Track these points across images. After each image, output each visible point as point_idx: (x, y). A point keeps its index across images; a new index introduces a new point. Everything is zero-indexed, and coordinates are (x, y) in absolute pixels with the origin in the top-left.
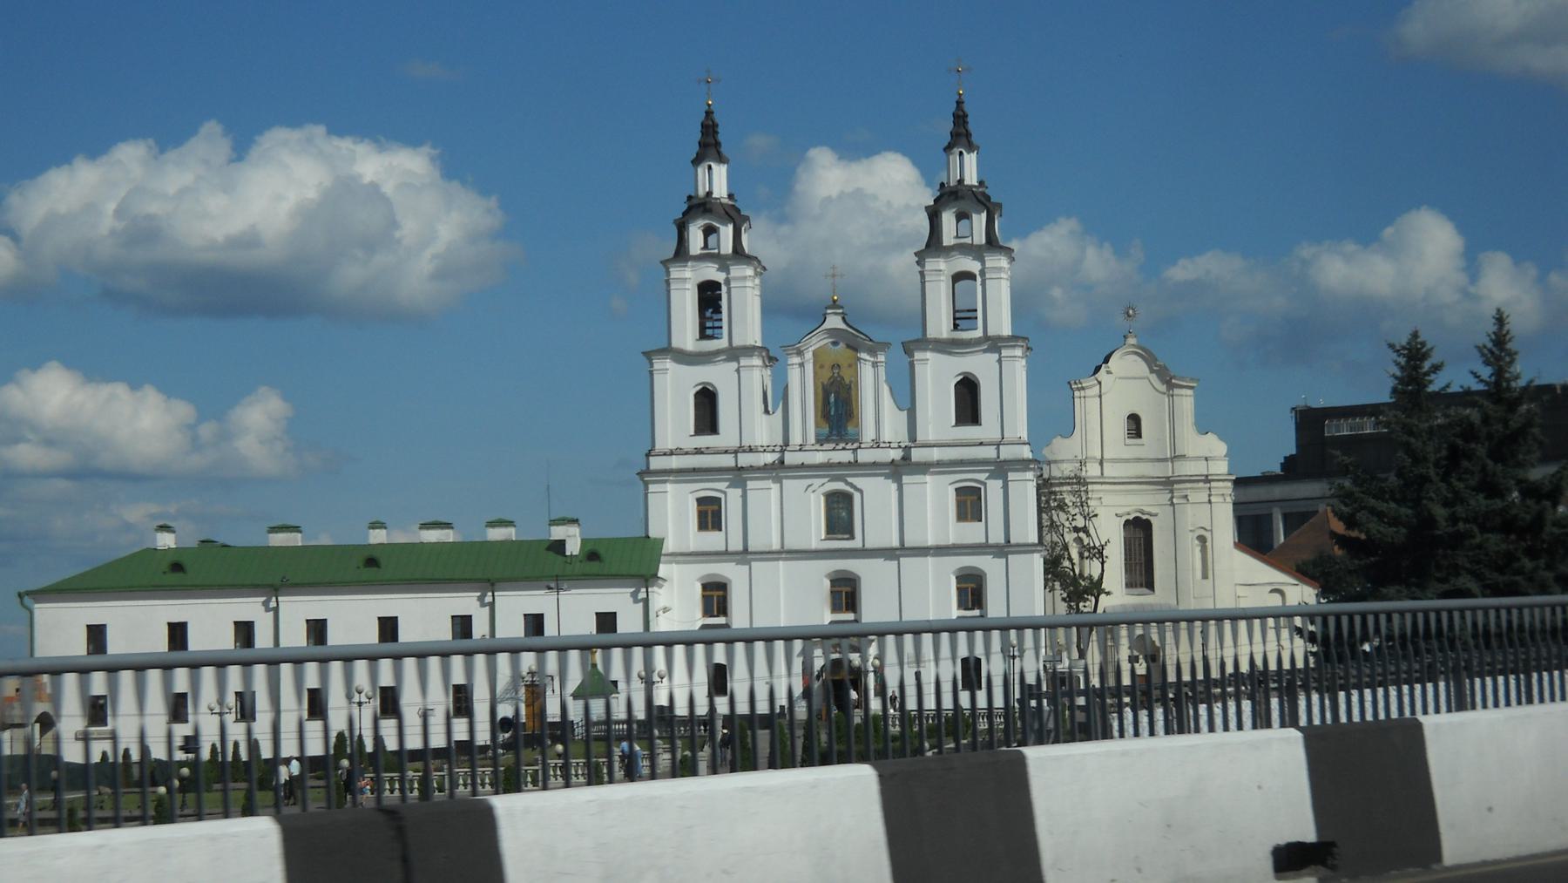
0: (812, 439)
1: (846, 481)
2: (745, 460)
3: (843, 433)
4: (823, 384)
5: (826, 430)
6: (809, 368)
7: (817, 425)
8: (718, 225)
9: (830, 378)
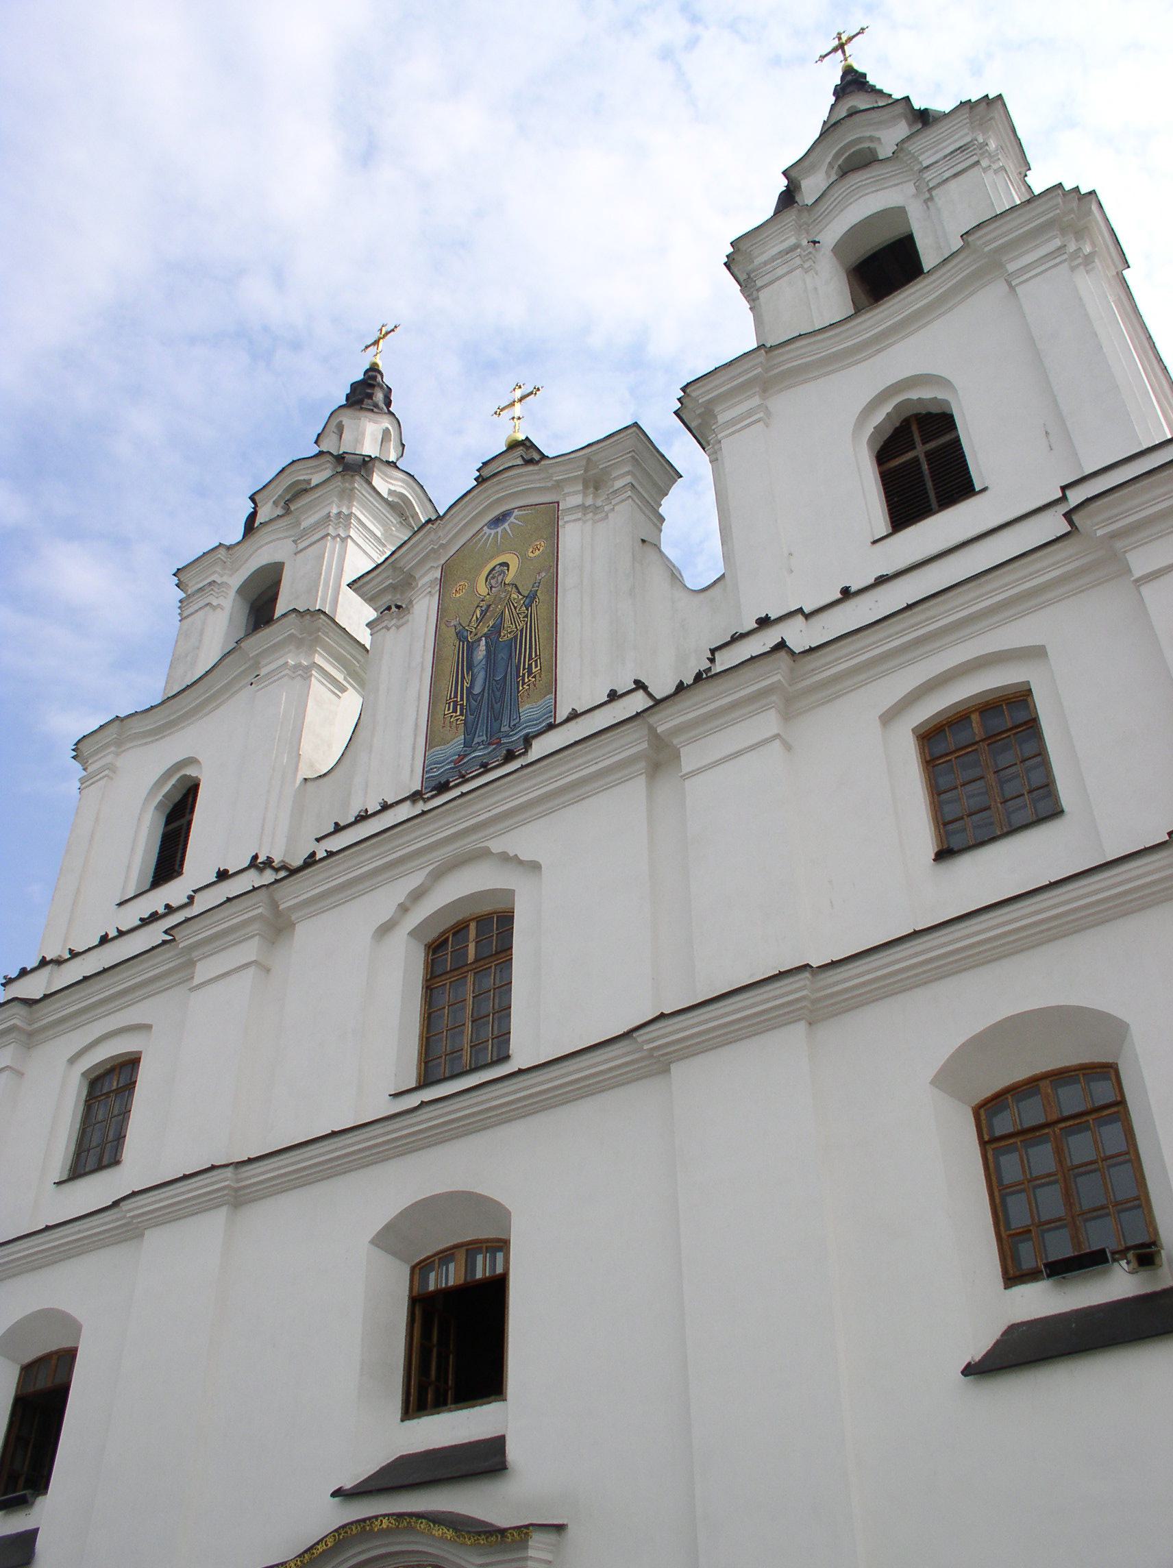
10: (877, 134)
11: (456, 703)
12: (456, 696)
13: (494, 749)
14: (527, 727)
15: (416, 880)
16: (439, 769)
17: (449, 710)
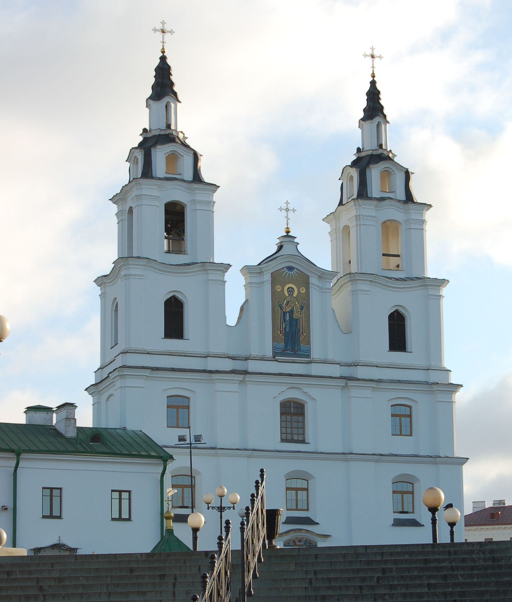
2: (212, 364)
5: (282, 345)
7: (274, 339)
8: (182, 154)
10: (396, 172)
11: (281, 330)
12: (281, 328)
13: (293, 353)
14: (302, 352)
16: (277, 350)
17: (279, 332)
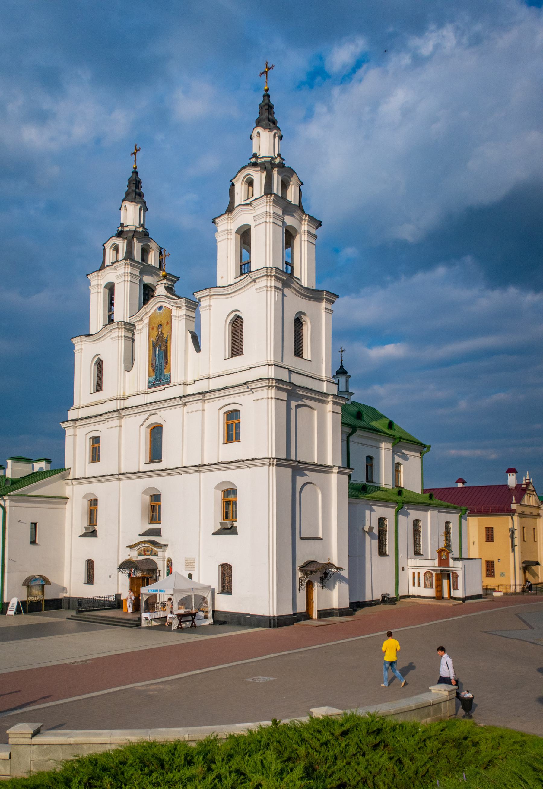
0: (143, 386)
1: (157, 414)
3: (162, 378)
4: (153, 341)
6: (146, 331)
9: (157, 337)
15: (146, 416)
